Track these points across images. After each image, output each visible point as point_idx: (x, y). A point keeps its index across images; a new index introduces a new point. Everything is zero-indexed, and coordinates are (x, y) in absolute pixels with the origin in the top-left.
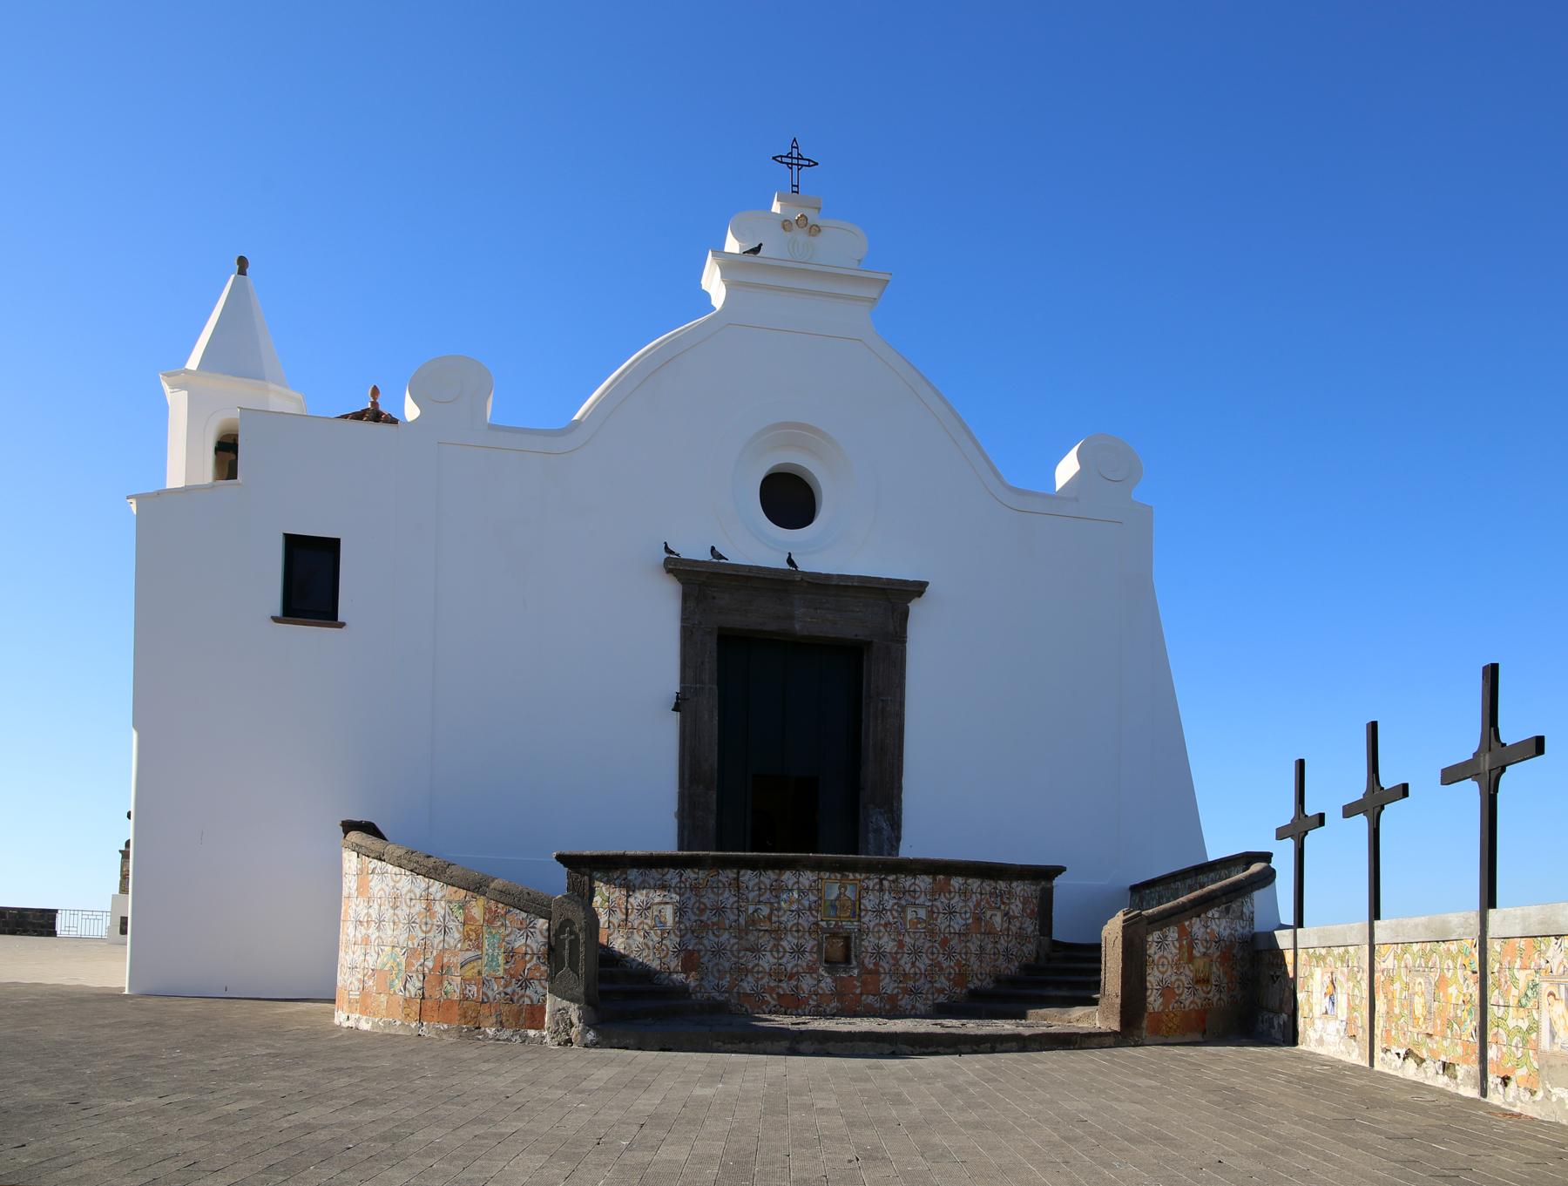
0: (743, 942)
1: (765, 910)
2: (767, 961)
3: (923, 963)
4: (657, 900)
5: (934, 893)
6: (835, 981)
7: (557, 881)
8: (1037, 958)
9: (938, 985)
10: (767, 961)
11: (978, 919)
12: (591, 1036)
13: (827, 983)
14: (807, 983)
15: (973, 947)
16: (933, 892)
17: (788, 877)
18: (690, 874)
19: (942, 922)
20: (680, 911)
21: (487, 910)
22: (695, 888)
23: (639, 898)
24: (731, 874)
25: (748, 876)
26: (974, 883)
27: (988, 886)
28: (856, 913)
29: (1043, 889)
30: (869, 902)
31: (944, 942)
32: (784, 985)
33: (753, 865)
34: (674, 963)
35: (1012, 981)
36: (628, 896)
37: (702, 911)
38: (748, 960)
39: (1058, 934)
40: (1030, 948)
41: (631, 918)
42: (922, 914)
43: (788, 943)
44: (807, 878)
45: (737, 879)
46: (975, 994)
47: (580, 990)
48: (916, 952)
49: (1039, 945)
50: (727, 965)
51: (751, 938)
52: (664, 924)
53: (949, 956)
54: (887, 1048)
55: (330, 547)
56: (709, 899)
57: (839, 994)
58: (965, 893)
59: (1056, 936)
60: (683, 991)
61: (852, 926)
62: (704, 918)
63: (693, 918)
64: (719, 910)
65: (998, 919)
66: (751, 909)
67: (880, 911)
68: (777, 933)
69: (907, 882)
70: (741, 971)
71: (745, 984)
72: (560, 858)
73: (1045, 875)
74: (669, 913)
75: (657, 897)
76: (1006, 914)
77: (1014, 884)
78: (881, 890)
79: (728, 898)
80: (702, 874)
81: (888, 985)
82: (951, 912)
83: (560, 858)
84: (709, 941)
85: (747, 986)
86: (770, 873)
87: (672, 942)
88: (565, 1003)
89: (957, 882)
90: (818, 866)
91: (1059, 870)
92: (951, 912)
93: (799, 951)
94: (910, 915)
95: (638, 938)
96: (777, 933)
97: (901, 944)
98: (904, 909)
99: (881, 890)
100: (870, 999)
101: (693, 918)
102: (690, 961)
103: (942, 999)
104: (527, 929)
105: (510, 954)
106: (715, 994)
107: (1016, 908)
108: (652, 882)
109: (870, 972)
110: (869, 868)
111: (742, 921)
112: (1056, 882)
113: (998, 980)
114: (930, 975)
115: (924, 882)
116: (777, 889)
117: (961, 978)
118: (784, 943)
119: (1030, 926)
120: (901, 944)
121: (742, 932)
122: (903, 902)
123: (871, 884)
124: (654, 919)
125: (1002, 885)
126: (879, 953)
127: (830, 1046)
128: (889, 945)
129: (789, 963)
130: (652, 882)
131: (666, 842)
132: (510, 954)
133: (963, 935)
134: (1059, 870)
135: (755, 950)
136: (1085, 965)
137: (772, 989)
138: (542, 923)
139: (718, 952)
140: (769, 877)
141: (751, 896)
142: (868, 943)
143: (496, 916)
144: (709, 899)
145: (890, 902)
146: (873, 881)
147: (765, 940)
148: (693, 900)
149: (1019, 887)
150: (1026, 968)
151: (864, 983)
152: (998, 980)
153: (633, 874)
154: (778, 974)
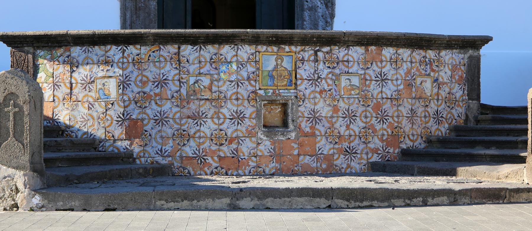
0: (185, 110)
1: (206, 81)
2: (209, 127)
3: (357, 126)
4: (101, 74)
5: (367, 63)
6: (273, 143)
8: (467, 119)
9: (372, 146)
10: (209, 127)
11: (409, 86)
12: (37, 200)
14: (247, 147)
15: (404, 111)
16: (366, 62)
17: (227, 50)
18: (132, 50)
19: (374, 89)
20: (124, 84)
22: (137, 62)
23: (82, 73)
24: (172, 49)
25: (187, 50)
26: (405, 53)
27: (418, 54)
28: (293, 80)
29: (470, 57)
30: (305, 71)
31: (377, 107)
32: (224, 148)
33: (193, 41)
34: (118, 132)
35: (443, 141)
36: (72, 72)
37: (144, 83)
38: (190, 126)
39: (486, 98)
40: (459, 111)
41: (75, 91)
42: (355, 81)
44: (246, 51)
45: (179, 53)
46: (406, 154)
47: (25, 159)
49: (468, 108)
50: (170, 132)
51: (193, 106)
52: (107, 96)
53: (383, 119)
54: (323, 202)
56: (151, 72)
57: (276, 155)
58: (395, 62)
59: (484, 100)
60: (127, 157)
62: (147, 89)
63: (136, 90)
65: (428, 86)
66: (192, 80)
67: (315, 80)
68: (218, 101)
69: (340, 52)
70: (183, 136)
71: (187, 149)
73: (474, 43)
74: (112, 86)
75: (100, 71)
76: (436, 80)
77: (443, 53)
78: (316, 61)
79: (170, 71)
80: (144, 50)
81: (324, 146)
84: (152, 110)
85: (188, 151)
86: (210, 47)
87: (116, 111)
88: (11, 171)
89: (388, 52)
90: (256, 40)
91: (486, 40)
92: (382, 79)
93: (239, 117)
94: (344, 82)
95: (83, 110)
97: (336, 109)
98: (338, 77)
99: (316, 61)
100: (307, 160)
101: (136, 90)
102: (134, 128)
103: (375, 158)
106: (159, 159)
107: (445, 74)
108: (95, 59)
109: (306, 135)
110: (305, 41)
111: (184, 91)
112: (484, 51)
113: (429, 141)
114: (364, 136)
115: (357, 52)
116: (216, 62)
117: (395, 137)
118: (224, 111)
119: (459, 92)
120: (336, 109)
121: (182, 102)
122: (337, 71)
123: (306, 55)
124: (98, 91)
125: (431, 54)
126: (315, 118)
127: (269, 202)
128: (325, 110)
129: (230, 129)
130: (95, 59)
131: (111, 23)
133: (395, 99)
134: (486, 40)
135: (197, 117)
136: (512, 126)
137: (214, 152)
139: (161, 120)
141: (192, 68)
142: (305, 109)
145: (324, 71)
146: (308, 53)
147: (207, 108)
148: (136, 73)
149: (447, 56)
150: (456, 129)
151: (301, 145)
152: (429, 141)
153: (76, 51)
154: (220, 138)
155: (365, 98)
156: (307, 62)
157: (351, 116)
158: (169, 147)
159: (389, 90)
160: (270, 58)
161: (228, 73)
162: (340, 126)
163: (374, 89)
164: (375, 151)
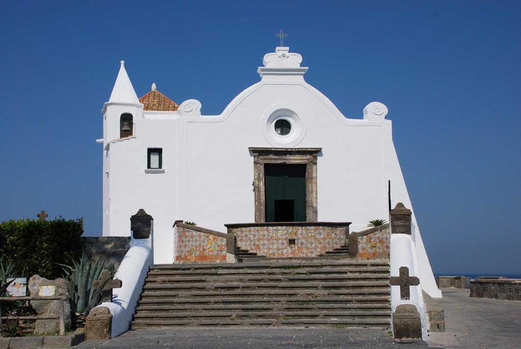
1: (274, 235)
3: (313, 246)
7: (225, 230)
10: (275, 246)
13: (290, 250)
14: (285, 251)
17: (280, 228)
18: (257, 228)
19: (318, 236)
21: (213, 237)
25: (270, 228)
28: (296, 234)
30: (299, 232)
38: (271, 246)
43: (280, 242)
44: (284, 228)
47: (233, 252)
48: (311, 243)
53: (320, 244)
55: (164, 172)
56: (261, 233)
61: (294, 238)
64: (264, 235)
65: (333, 235)
67: (302, 234)
68: (277, 240)
69: (309, 228)
70: (269, 249)
72: (225, 225)
79: (266, 232)
82: (320, 234)
83: (225, 225)
84: (262, 242)
85: (271, 252)
93: (283, 244)
94: (309, 235)
96: (277, 240)
99: (302, 229)
100: (300, 254)
103: (318, 254)
104: (222, 241)
105: (218, 246)
114: (315, 248)
121: (269, 240)
126: (302, 244)
128: (305, 242)
129: (281, 246)
132: (218, 246)
133: (324, 239)
138: (225, 239)
139: (264, 245)
140: (275, 228)
142: (300, 241)
143: (215, 238)
144: (261, 233)
154: (278, 249)
155: (316, 239)
156: (300, 230)
157: (311, 243)
158: (266, 251)
159: (322, 236)
160: (290, 229)
161: (280, 233)
162: (309, 245)
163: (318, 236)
164: (318, 252)
